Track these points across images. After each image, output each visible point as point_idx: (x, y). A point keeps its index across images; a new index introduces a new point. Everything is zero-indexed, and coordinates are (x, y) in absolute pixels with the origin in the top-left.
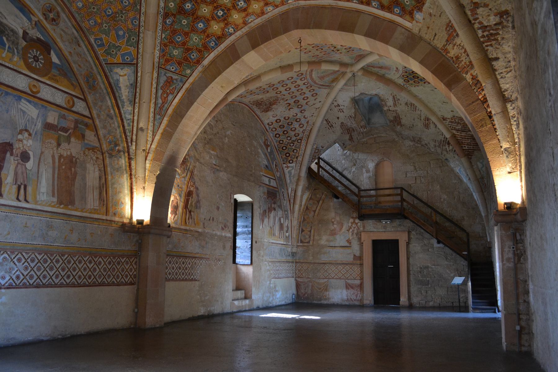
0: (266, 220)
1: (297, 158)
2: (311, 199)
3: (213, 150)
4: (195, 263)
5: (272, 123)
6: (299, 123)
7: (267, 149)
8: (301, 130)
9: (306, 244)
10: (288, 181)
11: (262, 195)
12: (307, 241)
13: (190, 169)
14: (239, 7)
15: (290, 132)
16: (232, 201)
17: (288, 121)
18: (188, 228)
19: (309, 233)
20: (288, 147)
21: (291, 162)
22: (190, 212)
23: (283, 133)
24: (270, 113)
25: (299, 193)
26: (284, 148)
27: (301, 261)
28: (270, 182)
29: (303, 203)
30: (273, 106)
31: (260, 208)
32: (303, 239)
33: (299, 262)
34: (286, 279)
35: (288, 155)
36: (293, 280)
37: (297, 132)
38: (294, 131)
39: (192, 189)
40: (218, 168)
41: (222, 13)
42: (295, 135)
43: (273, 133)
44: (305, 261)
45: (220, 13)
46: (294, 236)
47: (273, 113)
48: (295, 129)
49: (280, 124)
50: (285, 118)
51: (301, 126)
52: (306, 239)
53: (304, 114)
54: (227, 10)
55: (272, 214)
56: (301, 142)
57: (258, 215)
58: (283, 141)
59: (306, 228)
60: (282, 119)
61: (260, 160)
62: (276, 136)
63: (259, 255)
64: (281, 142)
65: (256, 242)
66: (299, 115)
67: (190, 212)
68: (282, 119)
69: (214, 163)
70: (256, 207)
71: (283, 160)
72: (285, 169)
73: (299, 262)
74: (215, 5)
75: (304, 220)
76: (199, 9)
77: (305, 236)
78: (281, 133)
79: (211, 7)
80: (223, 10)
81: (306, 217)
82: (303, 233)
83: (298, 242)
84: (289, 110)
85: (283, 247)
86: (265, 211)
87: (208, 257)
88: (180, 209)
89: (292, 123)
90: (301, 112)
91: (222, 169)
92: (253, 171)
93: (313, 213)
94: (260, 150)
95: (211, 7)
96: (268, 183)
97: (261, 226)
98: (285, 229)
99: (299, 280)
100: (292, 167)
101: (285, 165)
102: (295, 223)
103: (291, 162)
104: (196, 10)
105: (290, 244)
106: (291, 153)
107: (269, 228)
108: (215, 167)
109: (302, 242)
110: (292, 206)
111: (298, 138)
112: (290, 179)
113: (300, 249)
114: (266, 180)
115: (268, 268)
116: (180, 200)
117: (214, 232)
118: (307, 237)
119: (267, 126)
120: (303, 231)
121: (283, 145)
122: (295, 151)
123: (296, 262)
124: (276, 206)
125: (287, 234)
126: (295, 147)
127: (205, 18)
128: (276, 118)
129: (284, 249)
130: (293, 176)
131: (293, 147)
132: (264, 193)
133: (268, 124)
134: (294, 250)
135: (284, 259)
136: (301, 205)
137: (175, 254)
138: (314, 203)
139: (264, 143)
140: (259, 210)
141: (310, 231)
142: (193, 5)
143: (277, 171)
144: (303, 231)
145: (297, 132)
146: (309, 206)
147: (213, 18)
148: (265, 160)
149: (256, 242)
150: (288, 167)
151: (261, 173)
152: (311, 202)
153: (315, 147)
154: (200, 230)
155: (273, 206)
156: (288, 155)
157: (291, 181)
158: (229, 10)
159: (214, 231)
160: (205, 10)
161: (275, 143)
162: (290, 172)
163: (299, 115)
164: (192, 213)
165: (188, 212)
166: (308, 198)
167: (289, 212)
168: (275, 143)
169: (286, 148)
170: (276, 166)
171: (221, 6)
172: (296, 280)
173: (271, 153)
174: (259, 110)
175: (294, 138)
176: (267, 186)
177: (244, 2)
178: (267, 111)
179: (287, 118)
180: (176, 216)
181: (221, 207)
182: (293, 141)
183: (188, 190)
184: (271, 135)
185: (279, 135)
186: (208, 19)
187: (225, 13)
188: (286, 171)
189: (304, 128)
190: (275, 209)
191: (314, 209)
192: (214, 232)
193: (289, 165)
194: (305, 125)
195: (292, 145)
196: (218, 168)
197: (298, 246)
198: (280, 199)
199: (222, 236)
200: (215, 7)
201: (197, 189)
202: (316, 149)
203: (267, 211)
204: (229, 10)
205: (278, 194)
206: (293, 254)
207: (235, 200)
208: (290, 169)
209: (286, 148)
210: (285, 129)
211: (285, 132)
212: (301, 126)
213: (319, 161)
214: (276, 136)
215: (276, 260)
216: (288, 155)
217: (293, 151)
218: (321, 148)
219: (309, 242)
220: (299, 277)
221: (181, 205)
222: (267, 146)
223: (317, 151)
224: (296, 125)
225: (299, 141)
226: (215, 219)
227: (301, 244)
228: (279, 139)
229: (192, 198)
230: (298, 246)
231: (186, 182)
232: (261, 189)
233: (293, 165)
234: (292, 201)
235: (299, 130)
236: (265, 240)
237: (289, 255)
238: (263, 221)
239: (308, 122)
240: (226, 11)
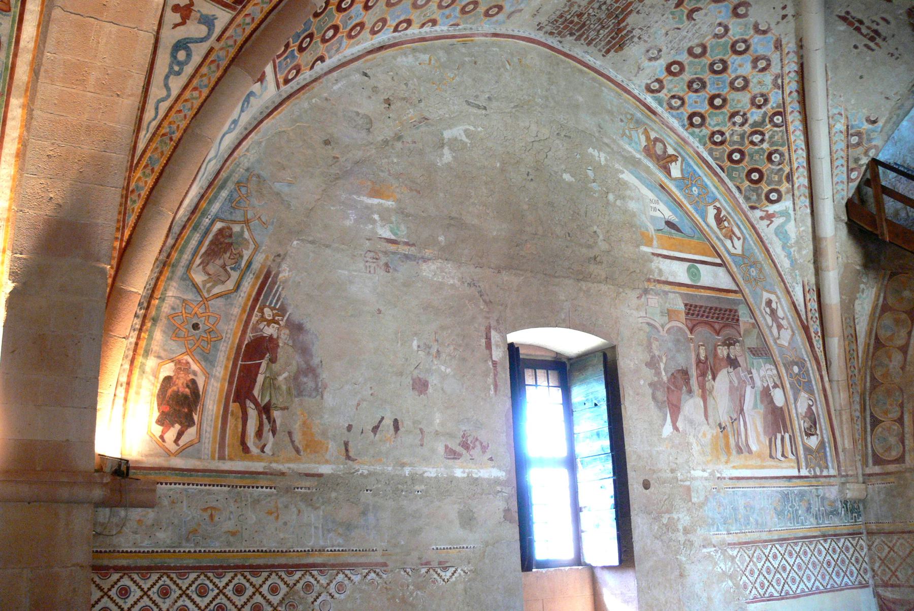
0: (692, 406)
1: (789, 178)
2: (885, 308)
3: (376, 193)
4: (308, 587)
5: (659, 81)
6: (748, 57)
7: (668, 173)
8: (768, 78)
9: (891, 468)
10: (784, 263)
11: (658, 320)
12: (894, 454)
13: (256, 266)
15: (733, 96)
16: (499, 354)
17: (706, 61)
18: (258, 466)
19: (896, 427)
20: (748, 149)
21: (773, 196)
22: (265, 410)
23: (711, 103)
24: (634, 51)
25: (833, 296)
26: (736, 156)
27: (886, 527)
28: (693, 273)
29: (862, 327)
30: (631, 20)
31: (652, 363)
32: (880, 451)
33: (880, 532)
34: (827, 597)
35: (755, 176)
36: (868, 591)
37: (755, 89)
38: (745, 87)
39: (270, 331)
40: (412, 251)
42: (753, 103)
43: (678, 118)
44: (900, 526)
46: (846, 443)
47: (642, 47)
48: (746, 80)
49: (687, 76)
50: (690, 51)
51: (762, 64)
52: (889, 449)
53: (751, 20)
55: (723, 381)
56: (785, 123)
57: (649, 391)
58: (722, 134)
59: (886, 412)
60: (684, 58)
61: (632, 205)
62: (692, 125)
63: (670, 527)
64: (717, 138)
65: (646, 485)
66: (736, 29)
67: (265, 410)
68: (684, 58)
69: (386, 233)
70: (627, 364)
71: (747, 199)
72: (762, 226)
73: (880, 532)
75: (875, 384)
77: (885, 439)
78: (704, 108)
81: (878, 375)
82: (879, 429)
83: (865, 464)
84: (690, 16)
85: (798, 487)
86: (685, 373)
87: (377, 558)
88: (211, 405)
89: (723, 62)
90: (736, 14)
91: (428, 253)
92: (603, 246)
93: (897, 357)
94: (627, 176)
96: (684, 278)
97: (668, 429)
98: (799, 424)
99: (888, 594)
100: (785, 213)
101: (758, 213)
102: (840, 398)
103: (773, 196)
105: (832, 472)
106: (766, 167)
107: (709, 432)
108: (392, 247)
109: (878, 461)
110: (818, 344)
111: (769, 108)
112: (789, 256)
113: (876, 488)
114: (679, 272)
115: (723, 566)
116: (208, 376)
117: (407, 471)
118: (893, 440)
119: (649, 99)
120: (875, 422)
121: (727, 148)
122: (776, 157)
123: (870, 533)
124: (735, 351)
125: (813, 442)
126: (772, 144)
128: (662, 63)
129: (802, 495)
130: (797, 242)
131: (765, 145)
132: (670, 314)
133: (649, 89)
134: (853, 491)
135: (809, 525)
136: (851, 337)
137: (191, 562)
138: (897, 321)
139: (648, 151)
140: (649, 373)
141: (900, 420)
143: (730, 235)
144: (875, 422)
145: (755, 89)
146: (884, 334)
148: (662, 206)
149: (646, 485)
150: (769, 217)
151: (645, 249)
152: (888, 319)
153: (840, 126)
154: (325, 469)
155: (722, 352)
156: (755, 176)
157: (793, 262)
159: (403, 465)
161: (701, 149)
162: (780, 232)
163: (736, 29)
164: (276, 414)
165: (252, 413)
166: (875, 308)
167: (811, 365)
168: (701, 149)
169: (742, 153)
170: (719, 220)
172: (877, 595)
173: (688, 180)
174: (591, 49)
175: (755, 115)
176: (684, 290)
178: (621, 48)
179: (698, 50)
180: (192, 432)
181: (433, 380)
182: (755, 124)
183: (250, 335)
184: (675, 123)
185: (702, 117)
188: (767, 231)
189: (775, 69)
190: (733, 363)
191: (901, 342)
192: (407, 471)
193: (772, 208)
194: (775, 57)
195: (757, 138)
196: (412, 251)
197: (867, 477)
198: (756, 325)
199: (451, 479)
201: (297, 328)
202: (848, 135)
203: (693, 372)
205: (743, 312)
206: (853, 508)
207: (513, 350)
208: (777, 221)
209: (742, 153)
210: (711, 90)
211: (718, 102)
212: (762, 64)
213: (876, 176)
214: (692, 125)
215: (765, 536)
216: (755, 176)
217: (769, 158)
218: (866, 126)
219: (901, 459)
220: (886, 585)
221: (214, 388)
222: (664, 161)
223: (854, 140)
224: (741, 66)
225: (778, 119)
226: (406, 424)
227: (877, 469)
228: (706, 132)
229: (273, 360)
230: (867, 477)
231: (236, 311)
232: (653, 301)
233: (786, 204)
234: (815, 327)
235: (762, 82)
236: (697, 473)
237: (834, 513)
238: (675, 410)
239: (778, 45)
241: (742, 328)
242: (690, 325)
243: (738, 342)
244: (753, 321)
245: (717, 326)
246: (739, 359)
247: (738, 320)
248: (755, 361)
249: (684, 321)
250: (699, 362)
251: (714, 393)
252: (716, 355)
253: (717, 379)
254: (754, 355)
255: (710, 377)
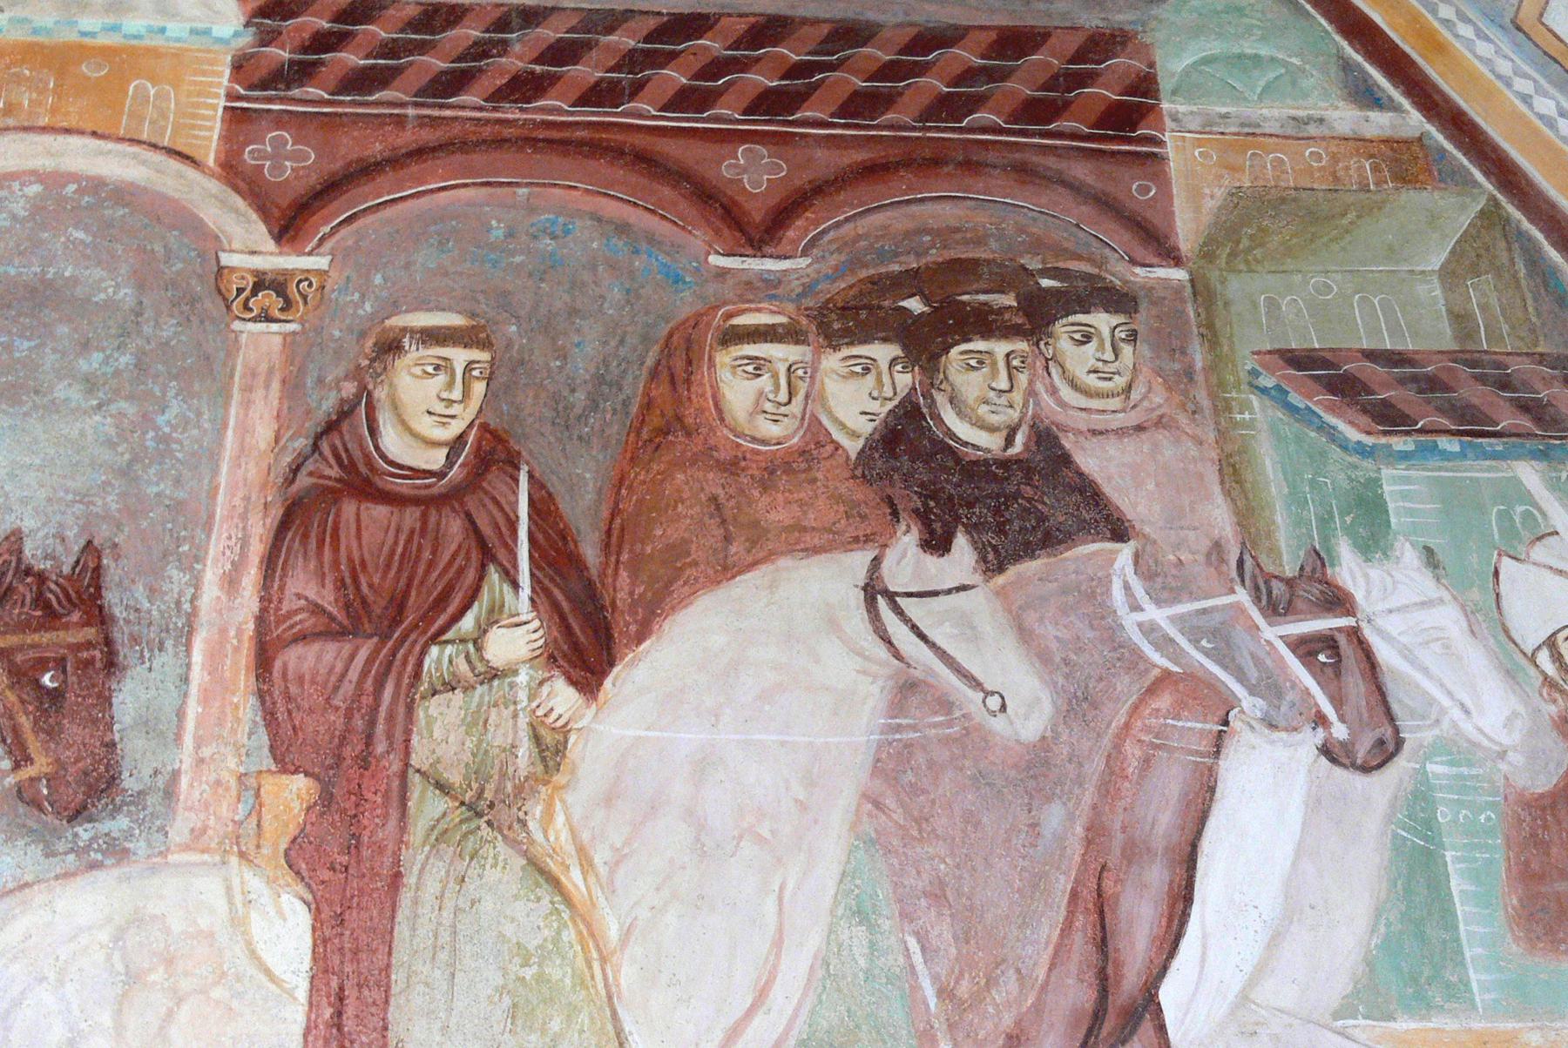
241: (1192, 186)
242: (290, 160)
243: (1120, 300)
244: (1414, 121)
245: (754, 173)
246: (1091, 460)
247: (1131, 115)
248: (1407, 485)
249: (209, 139)
250: (331, 482)
251: (554, 826)
252: (666, 413)
253: (639, 675)
254: (1389, 418)
255: (516, 640)
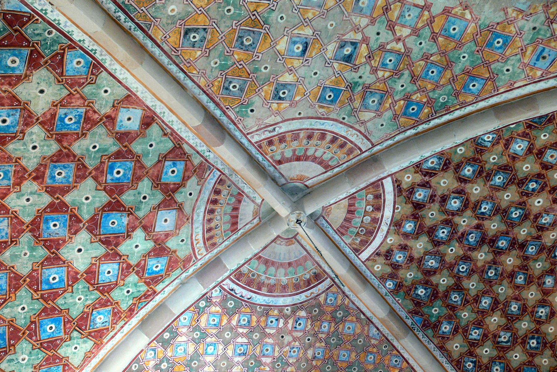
14: (544, 318)
41: (535, 341)
45: (533, 343)
54: (537, 333)
74: (519, 340)
76: (509, 361)
79: (519, 348)
80: (533, 338)
95: (519, 348)
104: (507, 365)
127: (525, 364)
142: (500, 363)
147: (532, 356)
158: (537, 331)
160: (516, 356)
171: (526, 336)
177: (543, 307)
186: (529, 362)
187: (538, 338)
200: (521, 343)
204: (537, 331)
240: (536, 336)
